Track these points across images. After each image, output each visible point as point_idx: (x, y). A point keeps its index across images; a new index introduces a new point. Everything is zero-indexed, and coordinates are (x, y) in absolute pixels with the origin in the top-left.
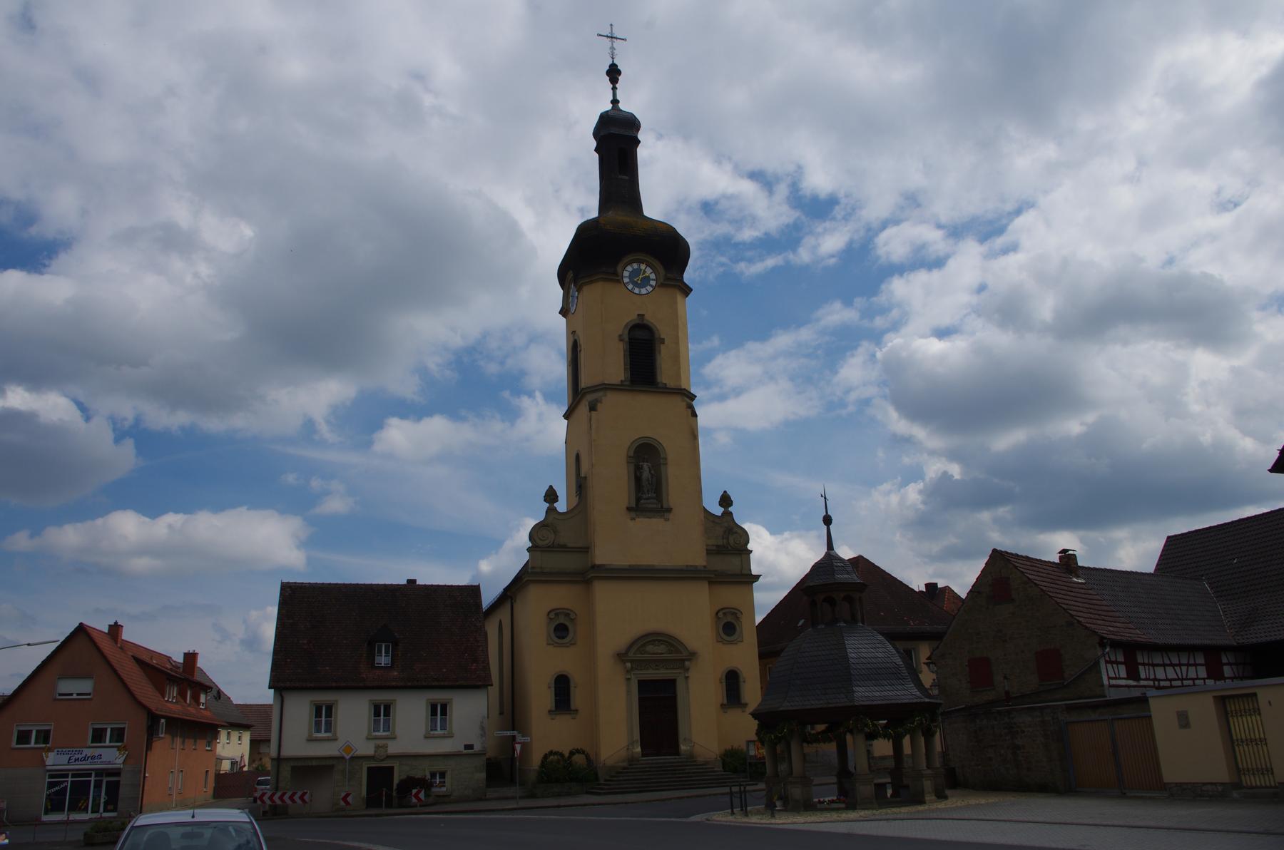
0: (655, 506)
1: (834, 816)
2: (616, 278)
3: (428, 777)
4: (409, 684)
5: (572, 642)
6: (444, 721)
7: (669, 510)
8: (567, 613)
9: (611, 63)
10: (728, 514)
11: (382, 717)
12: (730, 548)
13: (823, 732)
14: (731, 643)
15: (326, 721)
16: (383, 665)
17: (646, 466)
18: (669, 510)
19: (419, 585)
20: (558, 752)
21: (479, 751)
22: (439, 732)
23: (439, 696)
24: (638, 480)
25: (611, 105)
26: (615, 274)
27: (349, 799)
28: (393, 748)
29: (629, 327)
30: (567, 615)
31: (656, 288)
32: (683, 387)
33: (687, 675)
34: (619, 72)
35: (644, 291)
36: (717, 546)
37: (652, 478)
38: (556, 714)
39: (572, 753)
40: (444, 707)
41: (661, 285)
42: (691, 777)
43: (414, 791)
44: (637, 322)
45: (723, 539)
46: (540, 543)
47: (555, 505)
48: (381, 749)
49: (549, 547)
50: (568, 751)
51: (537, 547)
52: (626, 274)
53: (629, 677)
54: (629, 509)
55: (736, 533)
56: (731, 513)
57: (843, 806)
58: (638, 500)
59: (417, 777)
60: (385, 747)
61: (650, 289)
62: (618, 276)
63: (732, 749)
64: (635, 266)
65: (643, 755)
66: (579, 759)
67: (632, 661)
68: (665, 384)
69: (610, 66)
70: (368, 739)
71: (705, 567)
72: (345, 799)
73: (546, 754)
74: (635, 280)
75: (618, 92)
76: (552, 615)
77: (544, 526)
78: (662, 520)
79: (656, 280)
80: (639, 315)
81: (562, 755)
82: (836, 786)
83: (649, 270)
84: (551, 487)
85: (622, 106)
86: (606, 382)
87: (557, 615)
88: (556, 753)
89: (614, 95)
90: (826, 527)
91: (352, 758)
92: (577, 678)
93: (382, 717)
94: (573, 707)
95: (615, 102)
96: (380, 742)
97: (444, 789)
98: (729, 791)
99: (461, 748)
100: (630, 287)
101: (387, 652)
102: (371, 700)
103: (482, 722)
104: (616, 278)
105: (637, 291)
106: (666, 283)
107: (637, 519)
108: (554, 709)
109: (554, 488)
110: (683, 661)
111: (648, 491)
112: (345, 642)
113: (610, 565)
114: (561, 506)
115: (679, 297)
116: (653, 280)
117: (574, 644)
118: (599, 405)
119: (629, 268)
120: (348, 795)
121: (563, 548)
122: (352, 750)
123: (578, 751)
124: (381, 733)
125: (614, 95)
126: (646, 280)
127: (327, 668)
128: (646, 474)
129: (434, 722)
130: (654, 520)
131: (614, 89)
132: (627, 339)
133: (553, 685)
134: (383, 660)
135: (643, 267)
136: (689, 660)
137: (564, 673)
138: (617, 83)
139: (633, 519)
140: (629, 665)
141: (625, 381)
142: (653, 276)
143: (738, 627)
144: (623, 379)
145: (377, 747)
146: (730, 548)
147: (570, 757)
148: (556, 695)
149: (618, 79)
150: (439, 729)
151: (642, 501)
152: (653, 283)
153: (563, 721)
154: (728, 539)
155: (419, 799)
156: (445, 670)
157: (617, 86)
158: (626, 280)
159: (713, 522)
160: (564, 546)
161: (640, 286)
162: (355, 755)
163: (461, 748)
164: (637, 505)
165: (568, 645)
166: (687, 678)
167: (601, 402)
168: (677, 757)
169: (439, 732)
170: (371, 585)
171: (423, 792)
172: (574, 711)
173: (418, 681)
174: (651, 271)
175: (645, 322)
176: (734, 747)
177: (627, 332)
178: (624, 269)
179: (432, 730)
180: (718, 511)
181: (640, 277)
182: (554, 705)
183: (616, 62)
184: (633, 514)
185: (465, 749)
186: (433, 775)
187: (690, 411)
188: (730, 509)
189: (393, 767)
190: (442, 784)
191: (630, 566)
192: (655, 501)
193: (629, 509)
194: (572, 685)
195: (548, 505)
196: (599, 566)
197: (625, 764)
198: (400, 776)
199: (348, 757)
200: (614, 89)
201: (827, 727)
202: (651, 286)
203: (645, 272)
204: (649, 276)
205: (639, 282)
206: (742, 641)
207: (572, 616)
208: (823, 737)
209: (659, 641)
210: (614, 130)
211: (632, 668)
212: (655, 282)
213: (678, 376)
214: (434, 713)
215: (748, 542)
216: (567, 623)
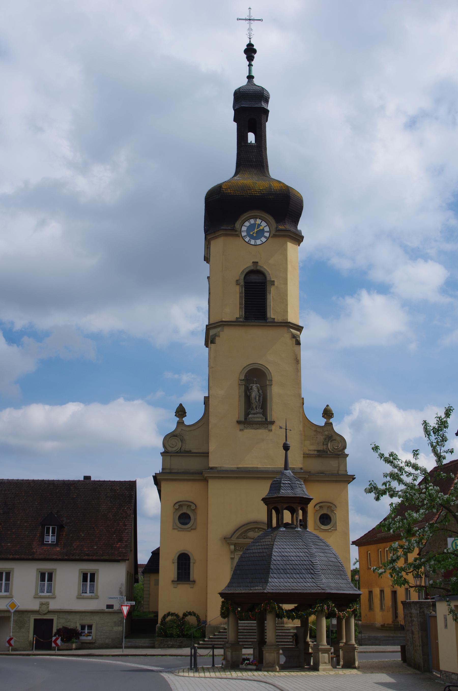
0: (260, 420)
1: (250, 673)
2: (236, 233)
3: (79, 628)
4: (66, 557)
6: (92, 586)
7: (272, 423)
8: (189, 504)
9: (248, 42)
10: (329, 425)
11: (46, 582)
12: (329, 452)
13: (292, 610)
15: (6, 584)
16: (50, 542)
17: (255, 387)
18: (272, 423)
19: (94, 481)
20: (174, 613)
21: (117, 610)
22: (88, 594)
23: (89, 567)
24: (248, 398)
25: (247, 80)
26: (234, 229)
27: (12, 642)
28: (54, 605)
29: (245, 273)
30: (189, 506)
31: (270, 238)
32: (289, 321)
34: (255, 51)
35: (259, 242)
36: (318, 451)
37: (259, 396)
38: (178, 584)
39: (185, 615)
40: (93, 576)
41: (274, 236)
43: (54, 638)
44: (252, 268)
45: (323, 445)
46: (170, 449)
47: (184, 419)
48: (44, 606)
49: (177, 452)
50: (182, 614)
51: (168, 452)
52: (244, 228)
53: (233, 557)
54: (239, 422)
55: (335, 440)
56: (331, 424)
57: (254, 667)
58: (247, 414)
59: (70, 628)
60: (47, 604)
61: (264, 240)
62: (236, 231)
64: (252, 221)
66: (191, 619)
67: (235, 545)
68: (274, 319)
69: (248, 46)
70: (35, 598)
71: (301, 469)
72: (9, 642)
73: (165, 615)
74: (251, 233)
75: (253, 68)
76: (177, 506)
77: (176, 436)
78: (267, 431)
79: (270, 232)
80: (253, 262)
81: (177, 616)
82: (400, 654)
83: (264, 224)
84: (181, 405)
85: (256, 81)
86: (224, 320)
87: (180, 506)
88: (173, 614)
89: (250, 71)
90: (285, 451)
91: (16, 611)
92: (195, 556)
93: (46, 582)
94: (191, 579)
95: (250, 77)
96: (44, 601)
97: (90, 638)
98: (215, 650)
99: (104, 608)
100: (247, 239)
101: (53, 532)
102: (38, 569)
103: (121, 588)
104: (236, 233)
105: (253, 242)
106: (277, 234)
107: (245, 430)
108: (176, 579)
111: (256, 407)
112: (26, 524)
113: (221, 467)
114: (189, 420)
115: (290, 246)
116: (267, 232)
117: (195, 529)
118: (217, 338)
119: (247, 224)
120: (11, 639)
121: (188, 453)
122: (16, 606)
123: (190, 614)
124: (45, 594)
125: (250, 71)
126: (261, 233)
127: (9, 544)
128: (254, 394)
129: (84, 586)
130: (260, 431)
131: (250, 65)
132: (242, 283)
133: (176, 561)
134: (50, 539)
135: (258, 221)
137: (186, 552)
138: (253, 60)
139: (241, 430)
140: (232, 547)
141: (240, 318)
142: (267, 229)
144: (238, 316)
145: (42, 604)
148: (178, 569)
149: (254, 57)
150: (88, 592)
151: (250, 416)
152: (267, 235)
153: (183, 588)
154: (327, 444)
155: (57, 644)
156: (95, 547)
157: (253, 63)
158: (244, 234)
159: (315, 431)
160: (190, 452)
161: (255, 238)
162: (17, 610)
163: (104, 608)
164: (245, 419)
165: (189, 529)
167: (219, 336)
169: (88, 594)
170: (53, 481)
171: (60, 639)
172: (192, 581)
173: (73, 555)
174: (266, 224)
175: (258, 268)
177: (243, 277)
178: (242, 225)
179: (83, 593)
180: (321, 422)
181: (256, 230)
182: (176, 576)
183: (252, 42)
184: (242, 426)
185: (107, 608)
186: (83, 627)
187: (294, 340)
188: (331, 420)
189: (52, 620)
190: (90, 634)
191: (238, 468)
192: (261, 416)
193: (239, 422)
194: (192, 561)
195: (178, 419)
196: (212, 468)
198: (57, 626)
199: (12, 611)
200: (250, 65)
201: (296, 607)
202: (265, 237)
203: (259, 225)
204: (263, 229)
205: (255, 235)
206: (336, 530)
207: (193, 507)
208: (290, 615)
209: (258, 528)
210: (245, 104)
211: (235, 550)
212: (269, 234)
213: (286, 311)
214: (85, 580)
215: (345, 447)
216: (189, 512)
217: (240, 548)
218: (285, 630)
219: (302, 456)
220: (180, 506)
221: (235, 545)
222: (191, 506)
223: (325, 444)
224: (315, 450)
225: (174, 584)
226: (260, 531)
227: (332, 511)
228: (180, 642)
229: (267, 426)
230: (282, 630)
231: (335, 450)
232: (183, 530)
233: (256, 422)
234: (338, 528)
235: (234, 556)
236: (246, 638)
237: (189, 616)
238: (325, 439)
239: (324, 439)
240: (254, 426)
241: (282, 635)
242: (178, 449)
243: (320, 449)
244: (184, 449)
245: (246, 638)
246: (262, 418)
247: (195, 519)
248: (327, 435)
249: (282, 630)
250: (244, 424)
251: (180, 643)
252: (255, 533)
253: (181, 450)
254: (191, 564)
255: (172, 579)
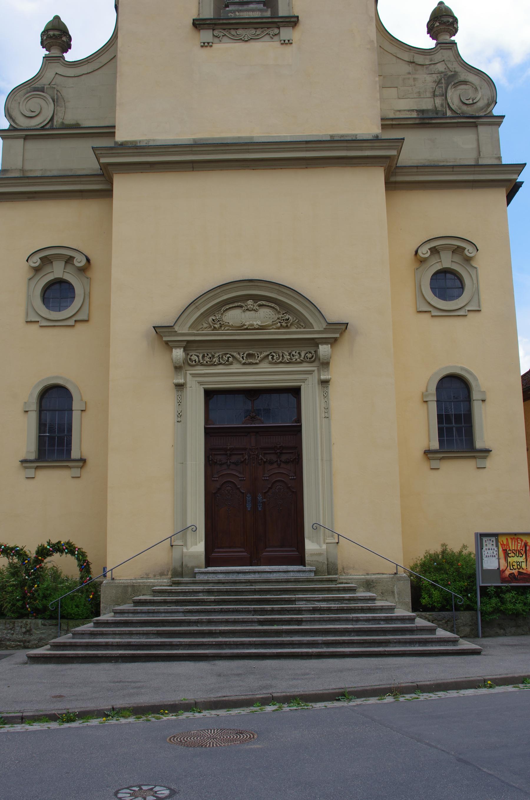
0: (257, 14)
5: (78, 317)
12: (449, 113)
14: (448, 314)
33: (323, 377)
38: (37, 468)
42: (299, 622)
45: (434, 96)
46: (23, 123)
47: (65, 54)
49: (43, 128)
53: (181, 381)
55: (465, 82)
63: (443, 552)
65: (209, 562)
67: (188, 346)
81: (20, 553)
109: (63, 20)
110: (315, 343)
123: (58, 548)
133: (34, 406)
136: (333, 342)
139: (205, 45)
140: (178, 353)
143: (467, 281)
146: (449, 113)
147: (37, 561)
154: (444, 95)
160: (77, 126)
165: (71, 322)
166: (325, 383)
168: (301, 568)
176: (449, 548)
184: (207, 35)
197: (163, 583)
207: (80, 262)
209: (256, 298)
215: (493, 101)
217: (203, 356)
218: (339, 590)
219: (379, 123)
220: (47, 261)
221: (188, 346)
222: (74, 258)
223: (436, 93)
224: (413, 110)
225: (26, 468)
226: (260, 306)
227: (468, 260)
228: (24, 630)
229: (276, 31)
230: (329, 590)
231: (465, 108)
232: (54, 324)
233: (246, 21)
234: (484, 307)
235: (185, 378)
236: (210, 622)
237: (56, 556)
238: (439, 83)
239: (435, 82)
240: (240, 32)
241: (329, 610)
242: (44, 121)
243: (424, 107)
244: (60, 121)
245: (210, 622)
246: (260, 10)
247: (87, 296)
248: (442, 73)
249: (329, 590)
250: (213, 30)
251: (25, 633)
252: (244, 311)
253: (53, 124)
254: (76, 415)
255: (23, 456)
